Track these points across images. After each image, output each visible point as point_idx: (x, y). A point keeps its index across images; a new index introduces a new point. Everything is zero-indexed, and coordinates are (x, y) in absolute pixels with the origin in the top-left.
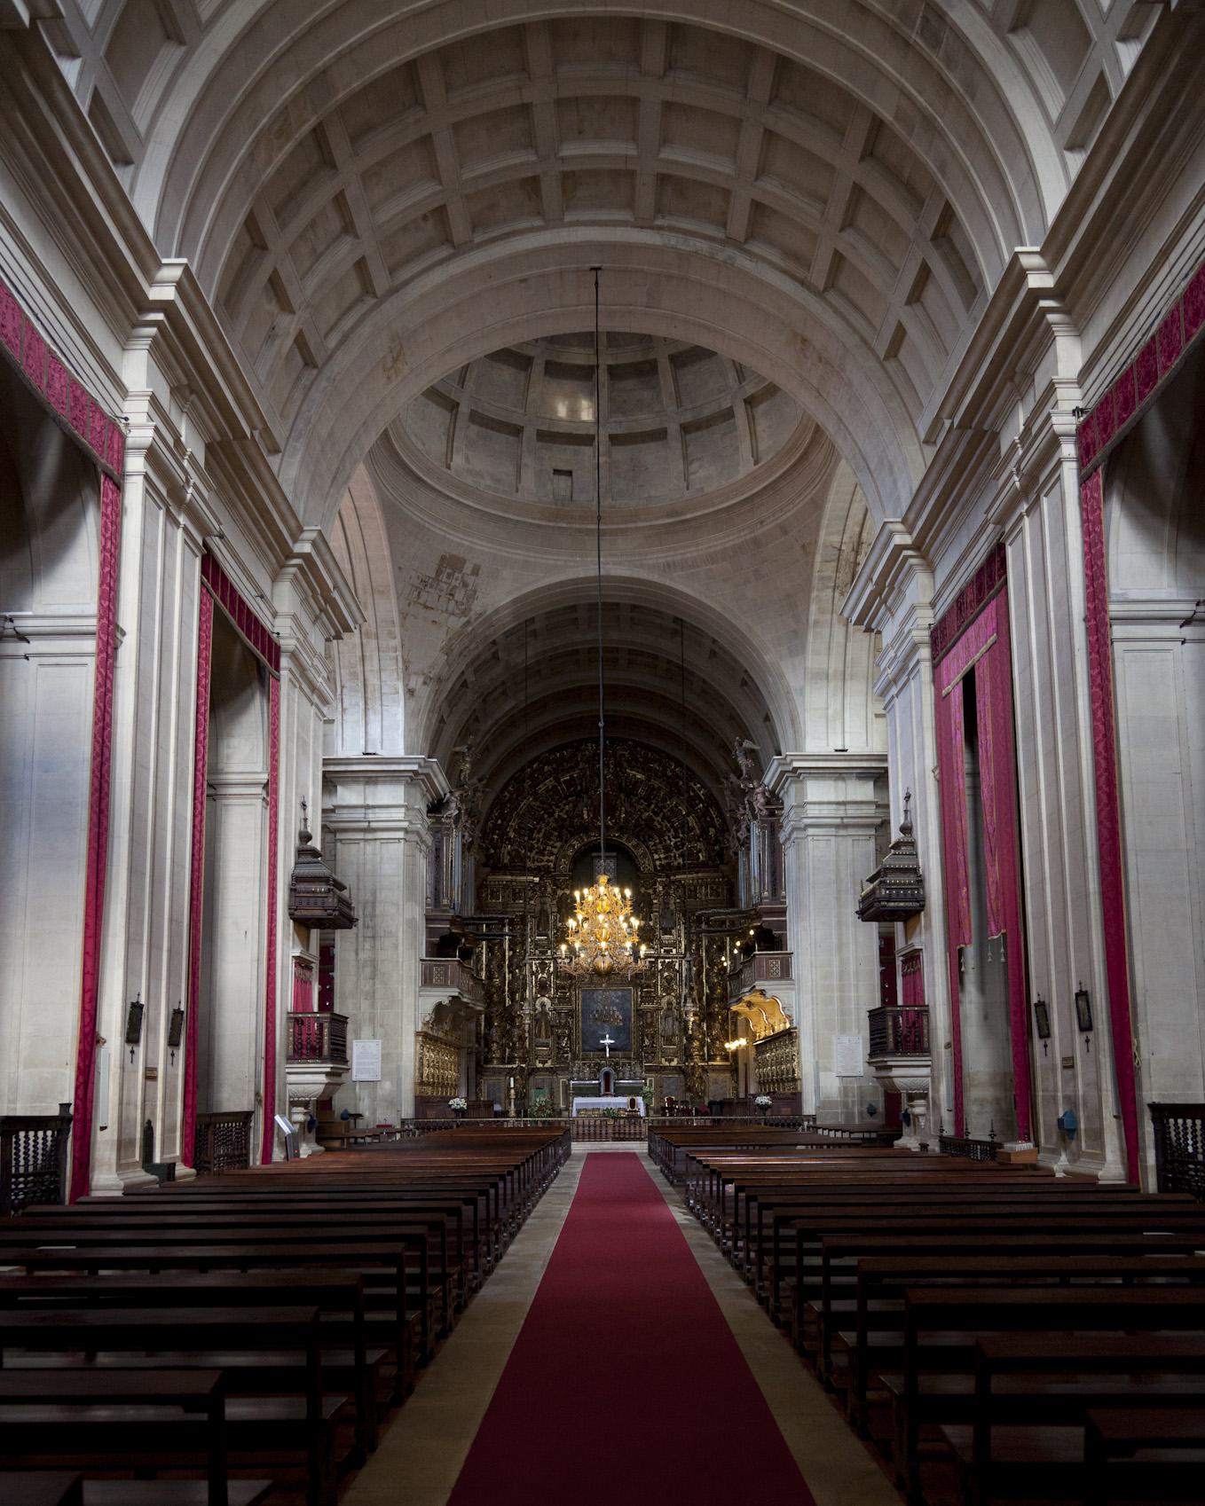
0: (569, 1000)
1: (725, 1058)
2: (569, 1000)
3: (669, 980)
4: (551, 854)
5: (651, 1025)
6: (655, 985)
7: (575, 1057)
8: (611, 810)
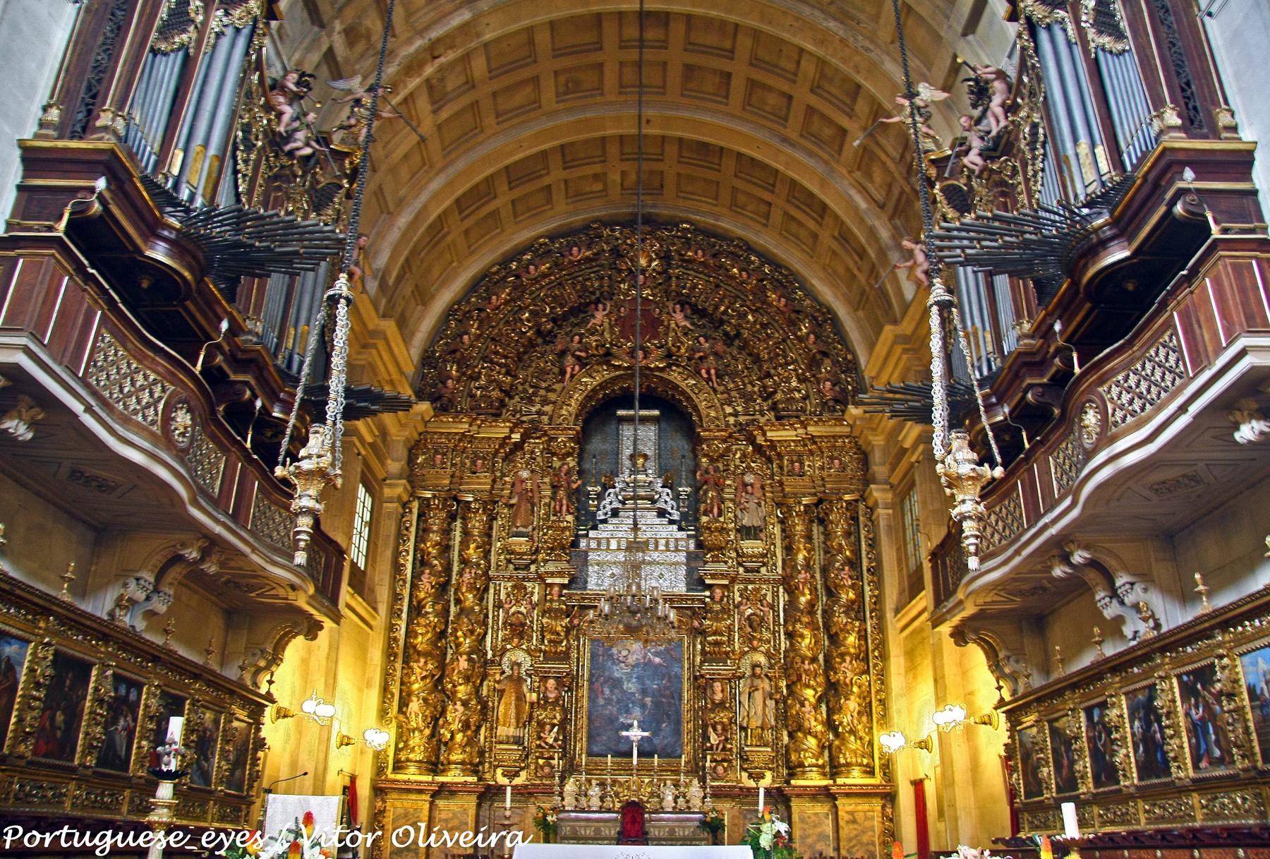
0: (565, 656)
1: (870, 772)
2: (565, 656)
3: (754, 623)
4: (545, 402)
5: (721, 705)
6: (730, 629)
7: (571, 768)
8: (653, 326)
